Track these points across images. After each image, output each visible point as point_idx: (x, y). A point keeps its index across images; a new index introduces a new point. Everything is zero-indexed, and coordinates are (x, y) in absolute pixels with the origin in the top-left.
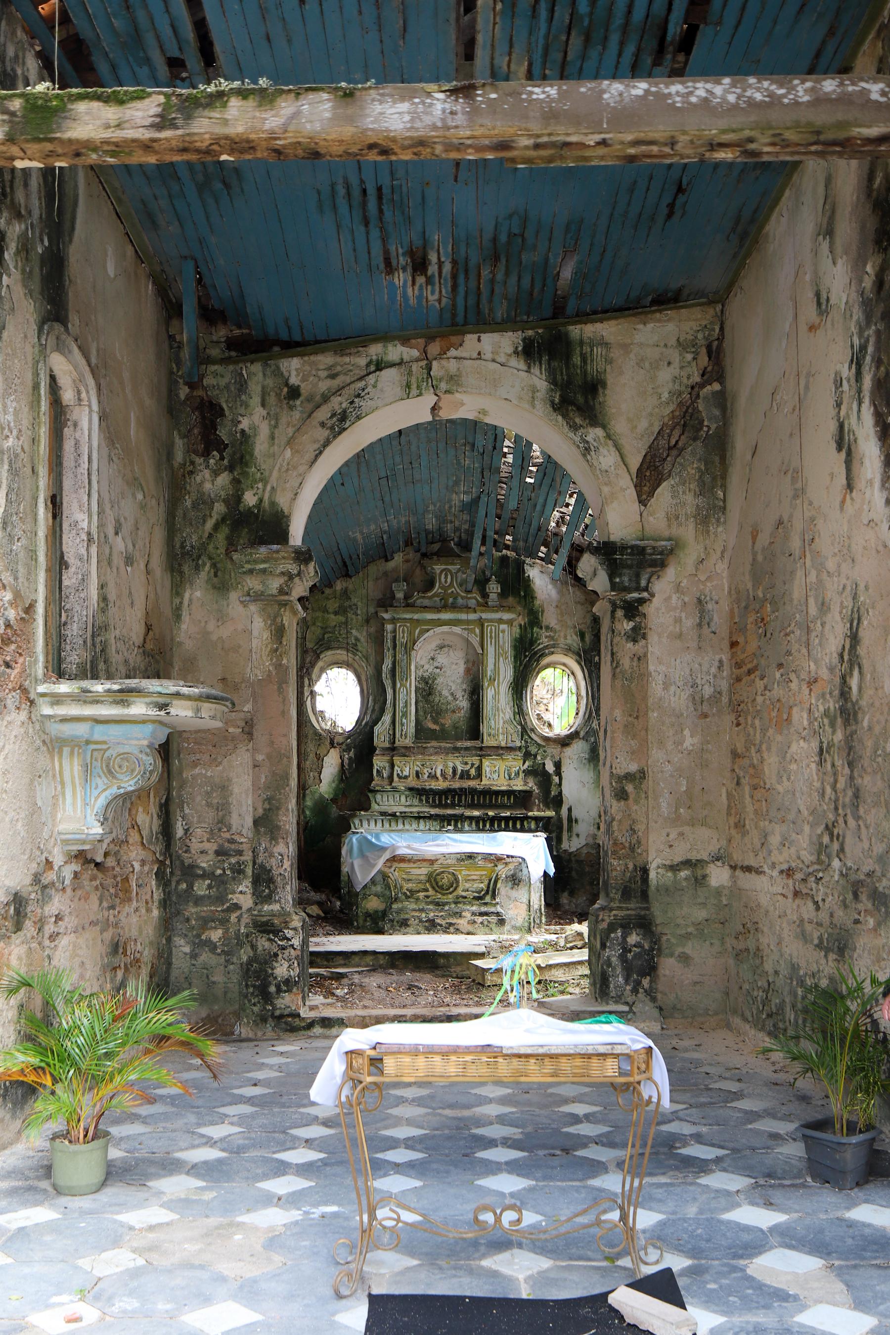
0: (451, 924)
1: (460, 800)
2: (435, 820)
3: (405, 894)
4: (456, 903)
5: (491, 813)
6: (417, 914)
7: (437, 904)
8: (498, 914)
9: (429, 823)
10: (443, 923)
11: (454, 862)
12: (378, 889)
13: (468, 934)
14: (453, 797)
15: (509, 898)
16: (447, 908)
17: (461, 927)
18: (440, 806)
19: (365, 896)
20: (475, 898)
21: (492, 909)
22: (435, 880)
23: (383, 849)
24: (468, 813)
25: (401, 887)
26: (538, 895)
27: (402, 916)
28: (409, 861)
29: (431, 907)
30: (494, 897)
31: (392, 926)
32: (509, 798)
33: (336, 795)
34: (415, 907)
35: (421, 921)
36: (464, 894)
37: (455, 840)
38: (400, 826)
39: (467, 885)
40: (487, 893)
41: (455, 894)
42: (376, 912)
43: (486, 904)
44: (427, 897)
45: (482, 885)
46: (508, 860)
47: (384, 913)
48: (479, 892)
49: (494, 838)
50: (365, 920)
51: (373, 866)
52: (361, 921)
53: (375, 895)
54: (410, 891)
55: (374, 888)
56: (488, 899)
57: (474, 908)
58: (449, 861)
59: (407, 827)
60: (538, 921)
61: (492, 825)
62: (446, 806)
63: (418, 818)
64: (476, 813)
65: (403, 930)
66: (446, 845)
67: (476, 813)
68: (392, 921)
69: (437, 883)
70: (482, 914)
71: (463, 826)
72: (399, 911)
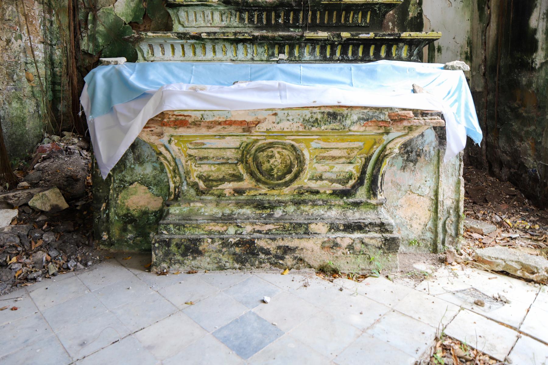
0: (287, 250)
1: (296, 19)
2: (261, 45)
3: (195, 185)
4: (297, 203)
5: (345, 35)
6: (218, 228)
7: (260, 205)
8: (382, 227)
9: (251, 50)
10: (272, 246)
11: (296, 126)
12: (148, 170)
13: (322, 270)
14: (287, 15)
15: (397, 186)
16: (278, 213)
17: (307, 256)
18: (269, 26)
19: (123, 185)
20: (336, 193)
21: (369, 216)
22: (255, 159)
23: (145, 96)
24: (309, 34)
25: (187, 173)
26: (452, 181)
27: (190, 233)
28: (196, 124)
29: (247, 211)
30: (373, 190)
31: (167, 254)
32: (364, 16)
33: (136, 17)
34: (217, 212)
35: (225, 244)
36: (314, 185)
37: (297, 78)
38: (210, 55)
39: (320, 168)
40: (360, 182)
41: (295, 185)
42: (145, 213)
43: (357, 205)
44: (239, 192)
45: (350, 168)
46: (415, 122)
47: (161, 214)
48: (345, 181)
49: (372, 73)
50: (124, 230)
51: (125, 131)
52: (115, 231)
53: (143, 182)
54: (206, 179)
55: (139, 170)
56: (361, 194)
57: (334, 213)
58: (285, 125)
59: (220, 55)
60: (451, 230)
61: (344, 52)
62: (277, 27)
63: (236, 42)
64: (323, 35)
65: (190, 262)
66: (281, 89)
67: (323, 35)
68: (168, 243)
69: (259, 166)
70: (350, 228)
71: (301, 54)
72: (179, 226)
